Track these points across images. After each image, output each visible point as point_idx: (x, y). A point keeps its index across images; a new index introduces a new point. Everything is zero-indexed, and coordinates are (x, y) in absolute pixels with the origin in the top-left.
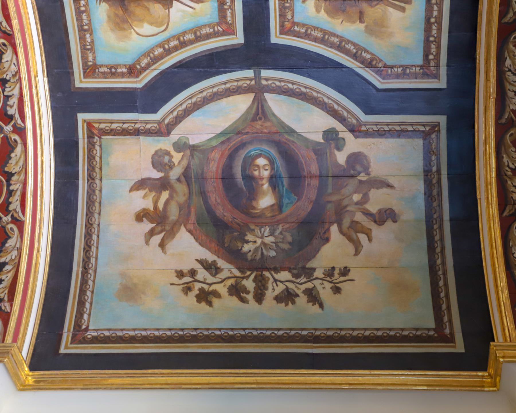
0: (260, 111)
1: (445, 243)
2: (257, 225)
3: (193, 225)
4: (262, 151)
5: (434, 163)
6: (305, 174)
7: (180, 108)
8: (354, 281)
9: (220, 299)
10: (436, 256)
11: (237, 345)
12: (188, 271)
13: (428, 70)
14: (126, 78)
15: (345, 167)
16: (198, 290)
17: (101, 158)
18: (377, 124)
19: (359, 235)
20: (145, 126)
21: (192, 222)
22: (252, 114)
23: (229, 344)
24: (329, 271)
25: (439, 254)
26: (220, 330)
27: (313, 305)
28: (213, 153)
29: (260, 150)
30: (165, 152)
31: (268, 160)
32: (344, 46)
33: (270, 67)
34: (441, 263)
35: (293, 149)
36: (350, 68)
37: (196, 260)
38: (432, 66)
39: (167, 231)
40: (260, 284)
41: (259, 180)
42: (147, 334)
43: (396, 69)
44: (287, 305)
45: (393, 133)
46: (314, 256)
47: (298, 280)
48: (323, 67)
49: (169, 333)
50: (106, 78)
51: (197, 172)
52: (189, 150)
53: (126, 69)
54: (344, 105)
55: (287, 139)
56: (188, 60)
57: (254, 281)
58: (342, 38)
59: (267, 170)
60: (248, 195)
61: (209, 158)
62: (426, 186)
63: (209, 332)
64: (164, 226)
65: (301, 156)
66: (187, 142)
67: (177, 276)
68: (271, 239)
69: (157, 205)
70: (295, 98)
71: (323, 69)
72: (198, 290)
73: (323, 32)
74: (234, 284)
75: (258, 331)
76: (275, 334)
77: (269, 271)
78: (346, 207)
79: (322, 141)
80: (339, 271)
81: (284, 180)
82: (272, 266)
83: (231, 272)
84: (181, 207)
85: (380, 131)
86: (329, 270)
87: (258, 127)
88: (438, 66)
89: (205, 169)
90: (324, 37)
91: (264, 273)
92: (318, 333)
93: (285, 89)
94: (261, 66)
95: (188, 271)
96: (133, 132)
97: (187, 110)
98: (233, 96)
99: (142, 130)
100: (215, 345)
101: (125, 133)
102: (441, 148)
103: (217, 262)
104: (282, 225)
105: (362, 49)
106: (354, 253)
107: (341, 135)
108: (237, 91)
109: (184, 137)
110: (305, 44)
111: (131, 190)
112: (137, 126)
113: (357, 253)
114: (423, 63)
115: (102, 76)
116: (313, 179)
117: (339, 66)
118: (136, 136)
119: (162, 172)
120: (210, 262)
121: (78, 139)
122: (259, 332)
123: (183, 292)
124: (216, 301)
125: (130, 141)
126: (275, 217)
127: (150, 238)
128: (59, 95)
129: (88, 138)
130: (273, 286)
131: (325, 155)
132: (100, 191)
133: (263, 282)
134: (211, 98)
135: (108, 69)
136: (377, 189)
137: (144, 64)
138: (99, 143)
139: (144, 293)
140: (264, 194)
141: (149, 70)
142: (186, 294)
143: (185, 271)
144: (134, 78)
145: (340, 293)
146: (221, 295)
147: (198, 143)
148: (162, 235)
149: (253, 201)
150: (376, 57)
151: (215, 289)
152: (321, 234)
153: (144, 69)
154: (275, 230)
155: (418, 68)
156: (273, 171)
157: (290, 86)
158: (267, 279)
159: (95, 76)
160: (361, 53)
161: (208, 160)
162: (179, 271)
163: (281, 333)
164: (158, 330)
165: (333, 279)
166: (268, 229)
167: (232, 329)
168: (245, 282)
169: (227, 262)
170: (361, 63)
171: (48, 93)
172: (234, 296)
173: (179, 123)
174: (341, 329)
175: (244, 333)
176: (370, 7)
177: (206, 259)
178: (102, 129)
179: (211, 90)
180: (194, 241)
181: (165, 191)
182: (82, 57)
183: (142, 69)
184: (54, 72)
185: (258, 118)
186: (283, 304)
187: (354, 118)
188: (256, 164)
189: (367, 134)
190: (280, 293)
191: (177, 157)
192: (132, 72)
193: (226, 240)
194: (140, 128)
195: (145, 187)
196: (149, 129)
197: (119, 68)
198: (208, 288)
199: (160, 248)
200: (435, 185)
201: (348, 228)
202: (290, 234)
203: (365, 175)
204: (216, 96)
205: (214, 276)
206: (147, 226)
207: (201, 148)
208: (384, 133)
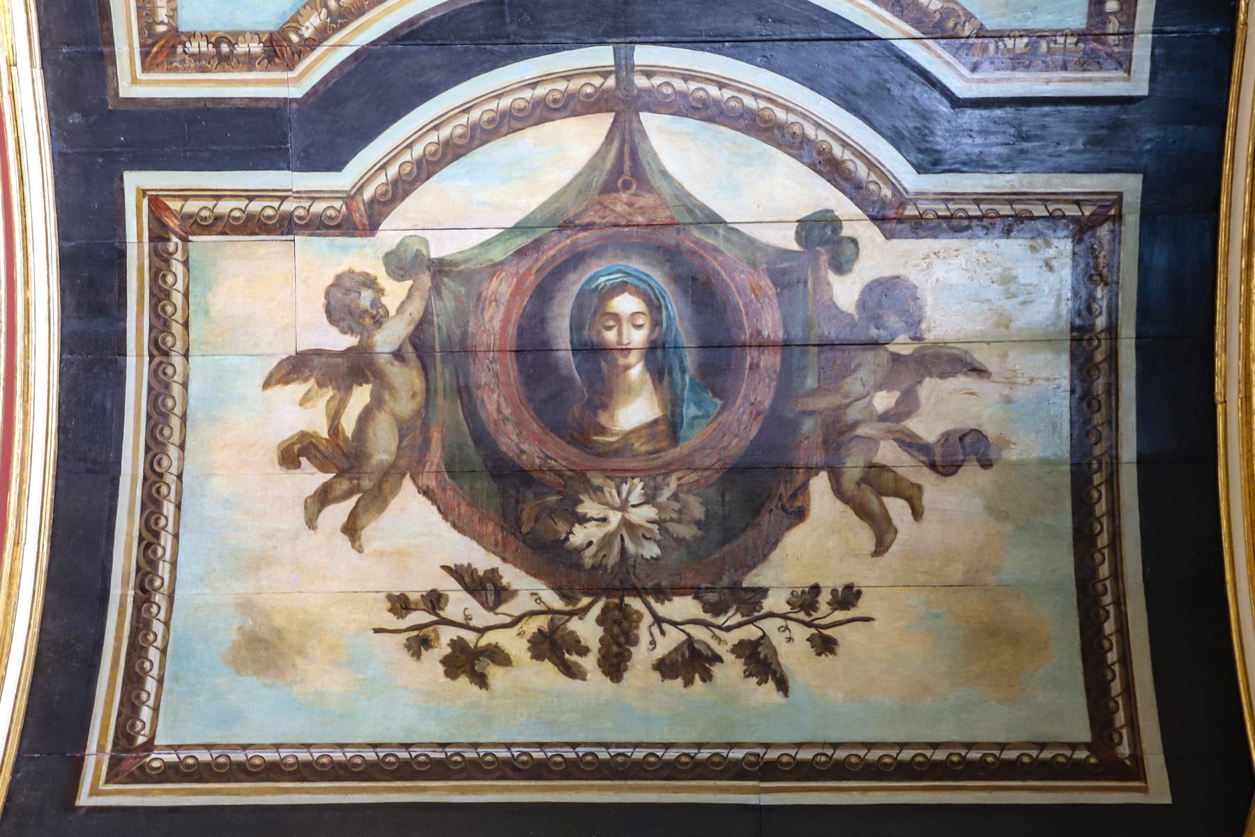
0: (627, 163)
1: (1122, 524)
2: (609, 474)
3: (437, 478)
4: (629, 274)
5: (1101, 307)
6: (746, 336)
7: (407, 157)
8: (870, 622)
9: (508, 668)
10: (1098, 557)
11: (556, 786)
12: (422, 596)
14: (261, 71)
15: (856, 317)
16: (449, 645)
17: (186, 295)
18: (948, 198)
19: (886, 500)
20: (310, 206)
21: (434, 468)
22: (604, 173)
23: (533, 783)
24: (804, 597)
25: (1106, 551)
26: (508, 746)
27: (759, 683)
28: (495, 282)
29: (625, 273)
30: (362, 279)
31: (644, 301)
33: (659, 38)
34: (1110, 576)
35: (714, 269)
36: (881, 39)
37: (443, 567)
38: (1111, 31)
39: (365, 492)
40: (616, 630)
41: (618, 354)
42: (311, 758)
43: (1009, 43)
44: (688, 682)
45: (991, 224)
46: (765, 557)
47: (720, 620)
48: (807, 36)
49: (370, 755)
50: (203, 70)
51: (449, 337)
52: (427, 273)
53: (262, 45)
54: (861, 147)
55: (697, 242)
56: (432, 17)
57: (600, 621)
59: (639, 327)
60: (586, 395)
61: (483, 294)
62: (1075, 369)
63: (478, 753)
64: (358, 479)
65: (734, 290)
66: (425, 252)
67: (392, 610)
68: (649, 512)
69: (339, 422)
70: (725, 125)
71: (806, 43)
72: (449, 645)
74: (546, 628)
75: (610, 750)
76: (657, 756)
77: (640, 596)
78: (855, 425)
79: (795, 247)
80: (830, 597)
81: (687, 354)
82: (650, 584)
83: (539, 600)
84: (403, 429)
85: (956, 218)
86: (803, 592)
87: (620, 208)
88: (1127, 35)
89: (471, 324)
91: (627, 600)
92: (773, 755)
94: (633, 35)
95: (422, 596)
96: (276, 223)
97: (424, 162)
98: (553, 120)
99: (300, 218)
100: (497, 786)
101: (253, 226)
102: (1121, 266)
103: (500, 573)
104: (679, 474)
106: (873, 548)
107: (846, 231)
108: (565, 107)
109: (415, 236)
111: (267, 384)
112: (288, 206)
113: (881, 547)
114: (1087, 23)
115: (192, 66)
116: (766, 352)
118: (282, 234)
119: (352, 334)
120: (481, 573)
121: (125, 243)
122: (613, 751)
123: (409, 651)
124: (495, 674)
125: (268, 248)
126: (658, 455)
127: (320, 511)
128: (75, 119)
129: (150, 241)
130: (652, 635)
131: (801, 285)
132: (185, 385)
133: (625, 624)
134: (492, 127)
135: (210, 45)
136: (942, 376)
137: (311, 30)
138: (183, 256)
139: (301, 652)
140: (630, 391)
141: (325, 48)
142: (417, 655)
143: (414, 597)
144: (282, 71)
145: (833, 652)
146: (512, 658)
147: (453, 254)
148: (351, 503)
149: (600, 412)
151: (494, 643)
152: (785, 500)
153: (310, 44)
154: (657, 489)
155: (1074, 39)
156: (657, 329)
157: (713, 91)
158: (635, 616)
159: (174, 64)
161: (478, 300)
162: (398, 596)
163: (672, 754)
164: (341, 746)
165: (815, 615)
166: (641, 485)
167: (541, 745)
168: (574, 625)
169: (527, 572)
170: (912, 25)
171: (43, 114)
172: (546, 660)
173: (403, 199)
174: (836, 746)
175: (573, 755)
177: (469, 565)
178: (190, 216)
179: (493, 105)
180: (438, 517)
181: (361, 385)
182: (139, 9)
183: (305, 46)
184: (62, 52)
185: (620, 182)
186: (680, 681)
187: (885, 184)
188: (611, 311)
189: (920, 226)
190: (670, 653)
191: (394, 292)
192: (275, 52)
193: (524, 516)
194: (296, 213)
195: (307, 372)
196: (319, 216)
197: (243, 43)
198: (475, 641)
199: (346, 538)
200: (1101, 366)
201: (858, 484)
202: (701, 500)
203: (910, 341)
204: (506, 120)
205: (492, 608)
206: (311, 479)
207: (462, 267)
208: (966, 223)
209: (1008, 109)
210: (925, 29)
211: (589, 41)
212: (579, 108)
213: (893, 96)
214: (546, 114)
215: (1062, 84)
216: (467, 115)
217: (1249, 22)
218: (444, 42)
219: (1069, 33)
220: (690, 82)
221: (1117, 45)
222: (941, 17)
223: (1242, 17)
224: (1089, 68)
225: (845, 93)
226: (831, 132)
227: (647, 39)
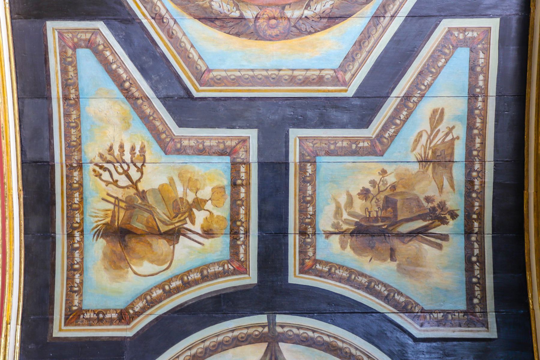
13: (473, 316)
14: (115, 325)
32: (374, 287)
33: (287, 312)
38: (477, 311)
43: (435, 315)
48: (349, 311)
50: (91, 325)
53: (117, 314)
56: (190, 303)
58: (370, 278)
70: (316, 348)
71: (349, 314)
73: (349, 271)
88: (485, 313)
90: (350, 277)
93: (305, 337)
98: (241, 346)
105: (395, 291)
108: (246, 340)
110: (328, 285)
114: (467, 308)
115: (86, 323)
117: (368, 311)
128: (31, 346)
134: (214, 349)
135: (95, 315)
137: (139, 308)
141: (144, 316)
144: (125, 325)
150: (411, 301)
153: (138, 314)
155: (462, 314)
157: (310, 334)
159: (78, 323)
160: (394, 296)
170: (393, 307)
171: (18, 345)
176: (402, 243)
182: (66, 300)
183: (136, 315)
184: (31, 318)
192: (122, 317)
197: (109, 314)
209: (438, 343)
210: (399, 309)
211: (257, 313)
212: (252, 341)
213: (388, 337)
214: (238, 343)
215: (460, 332)
216: (204, 344)
217: (534, 309)
218: (195, 313)
219: (460, 312)
220: (300, 330)
221: (481, 317)
222: (405, 304)
223: (531, 307)
224: (471, 326)
225: (367, 335)
226: (362, 351)
227: (281, 312)
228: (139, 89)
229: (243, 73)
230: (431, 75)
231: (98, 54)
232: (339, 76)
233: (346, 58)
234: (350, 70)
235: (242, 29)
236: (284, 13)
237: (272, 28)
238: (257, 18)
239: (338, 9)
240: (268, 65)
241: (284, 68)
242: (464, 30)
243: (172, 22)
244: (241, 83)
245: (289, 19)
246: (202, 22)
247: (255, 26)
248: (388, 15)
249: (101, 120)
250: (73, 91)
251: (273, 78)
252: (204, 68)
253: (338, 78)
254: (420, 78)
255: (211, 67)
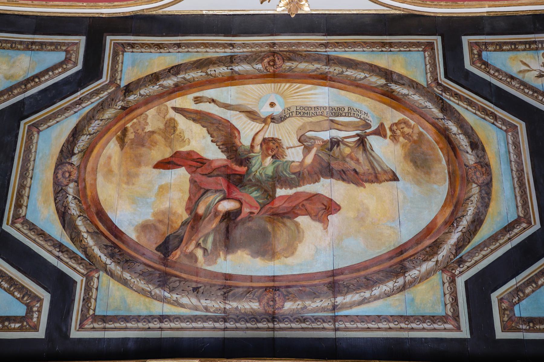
228: (32, 87)
229: (33, 154)
230: (8, 287)
231: (61, 64)
232: (20, 219)
233: (33, 224)
234: (23, 227)
235: (64, 154)
236: (72, 182)
237: (63, 174)
238: (71, 164)
239: (70, 219)
240: (37, 171)
241: (32, 181)
242: (39, 311)
243: (76, 110)
244: (26, 153)
245: (67, 185)
246: (74, 129)
247: (66, 163)
248: (60, 254)
249: (14, 63)
250: (37, 47)
251: (26, 174)
252: (40, 128)
253: (19, 218)
254: (8, 278)
255: (41, 133)
